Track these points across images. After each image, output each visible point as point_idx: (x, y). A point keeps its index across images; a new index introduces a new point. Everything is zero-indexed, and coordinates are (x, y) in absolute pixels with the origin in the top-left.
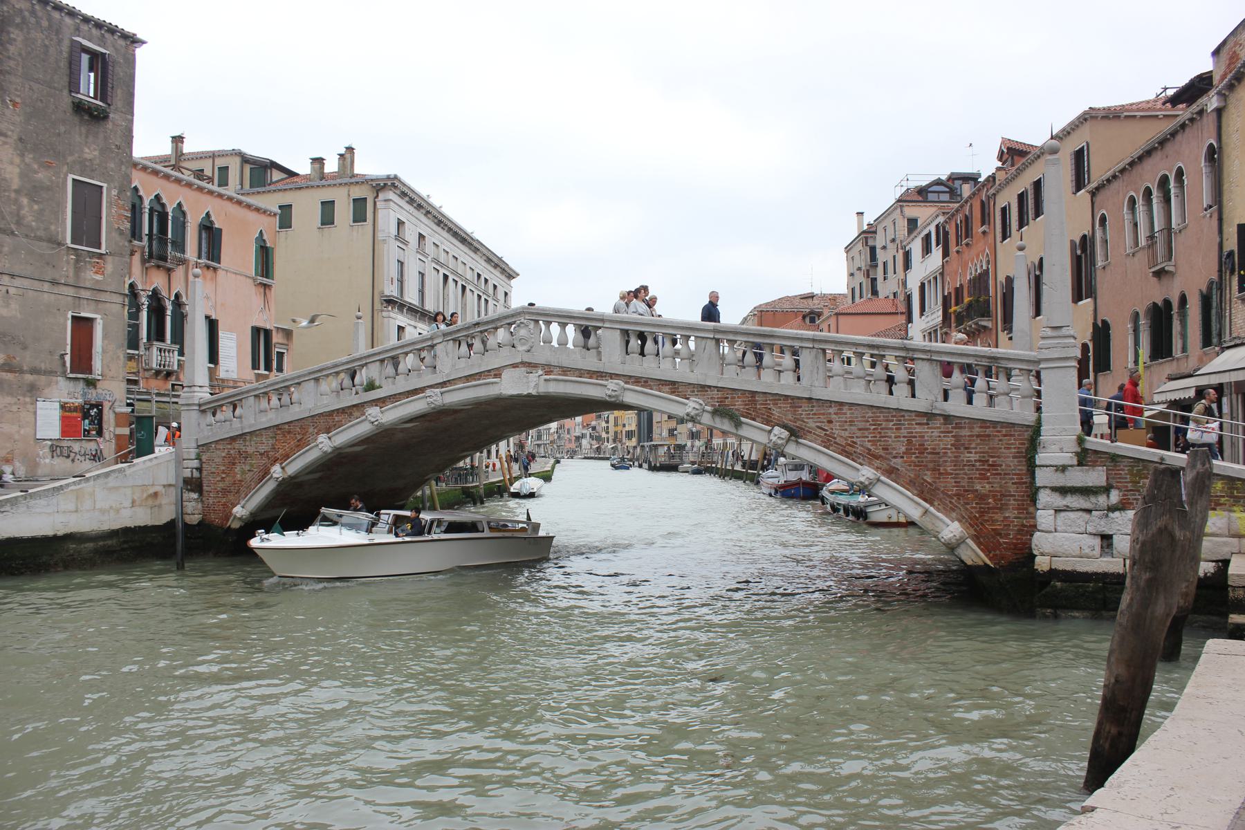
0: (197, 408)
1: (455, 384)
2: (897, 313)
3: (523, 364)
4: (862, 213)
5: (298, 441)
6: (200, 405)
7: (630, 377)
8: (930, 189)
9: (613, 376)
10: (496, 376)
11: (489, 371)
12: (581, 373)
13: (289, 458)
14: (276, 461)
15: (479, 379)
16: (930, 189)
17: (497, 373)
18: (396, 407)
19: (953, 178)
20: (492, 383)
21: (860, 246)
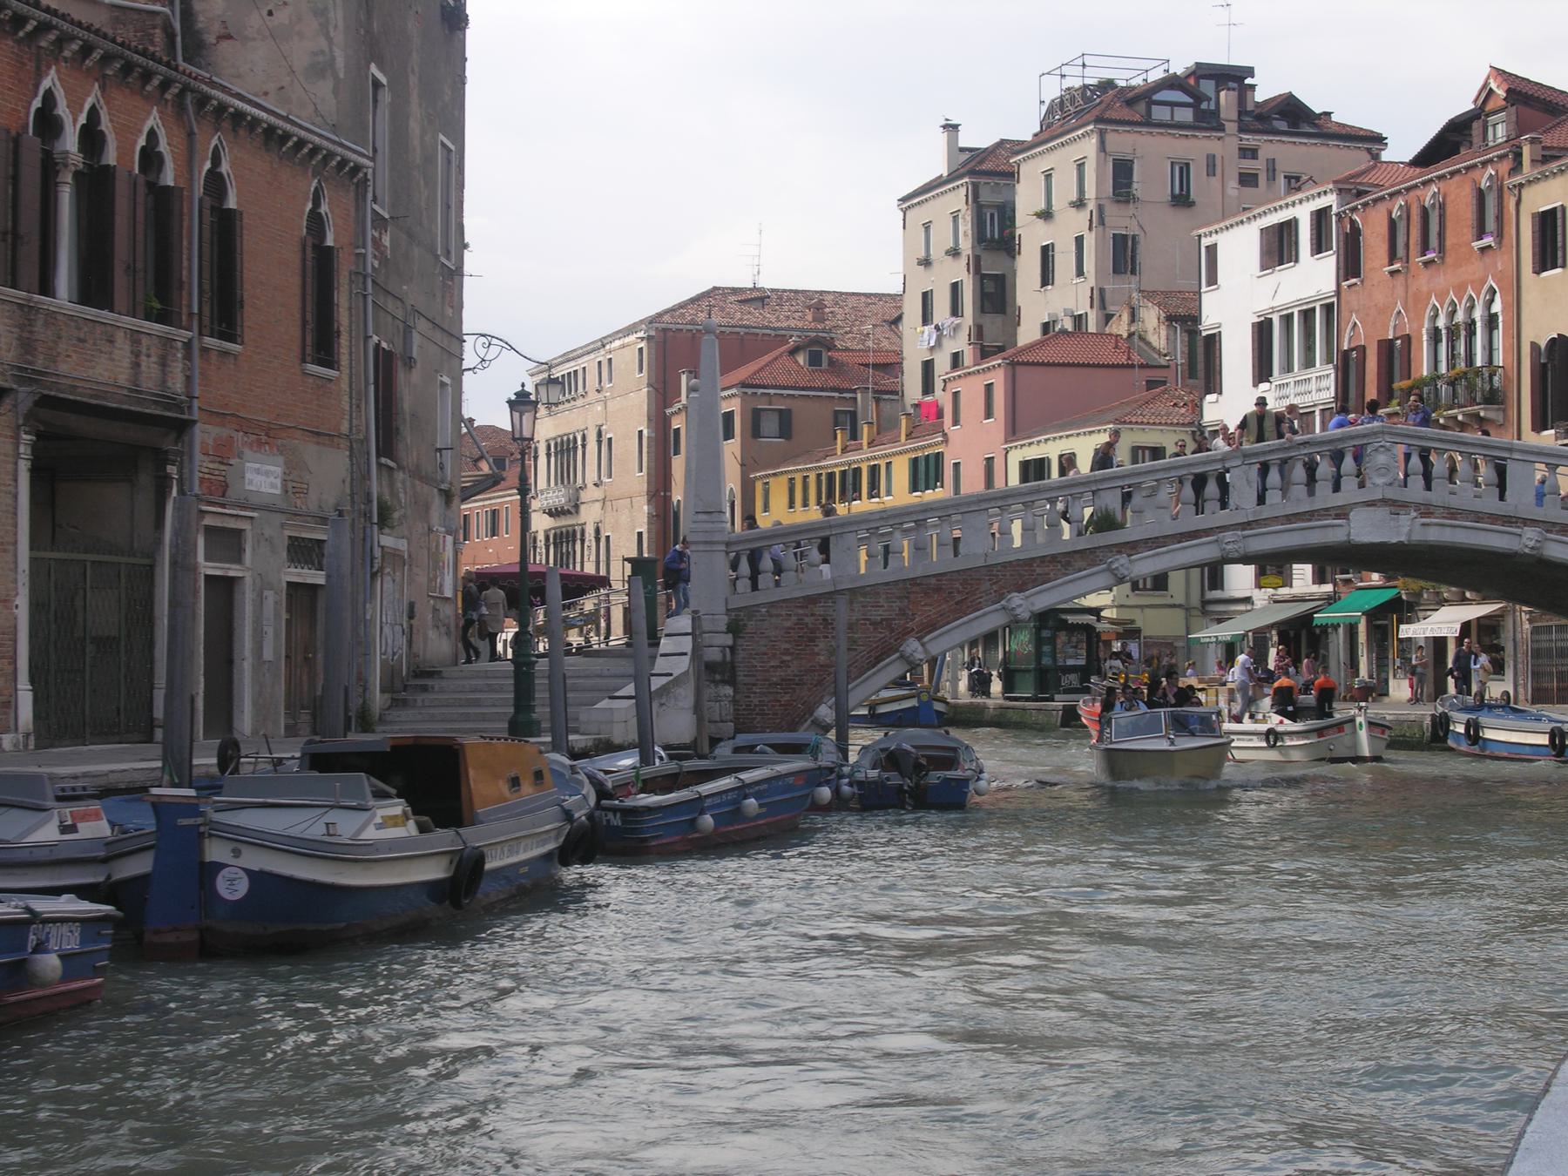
0: (723, 548)
1: (1266, 526)
2: (1133, 366)
3: (1385, 502)
4: (955, 127)
5: (957, 603)
6: (728, 544)
7: (1554, 524)
8: (1156, 97)
9: (1527, 522)
10: (1338, 517)
11: (1327, 509)
12: (1478, 516)
13: (936, 629)
14: (906, 633)
15: (1310, 520)
16: (1156, 97)
17: (1342, 513)
18: (1158, 554)
19: (1203, 71)
20: (1333, 526)
21: (957, 199)
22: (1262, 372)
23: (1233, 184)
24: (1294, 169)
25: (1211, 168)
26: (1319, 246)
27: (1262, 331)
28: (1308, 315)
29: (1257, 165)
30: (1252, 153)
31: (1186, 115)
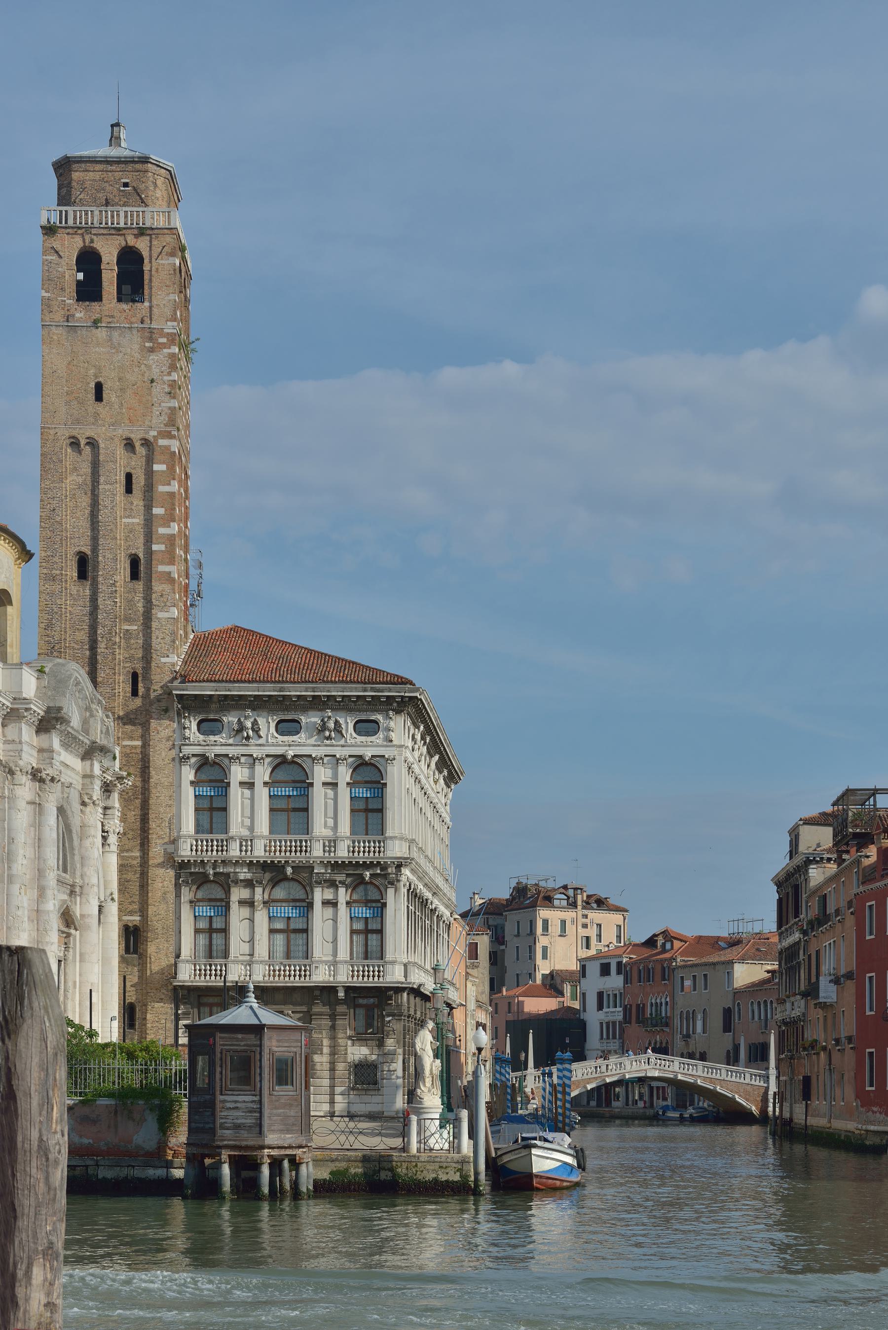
22: (600, 1007)
23: (580, 927)
24: (599, 922)
25: (573, 921)
26: (619, 972)
27: (600, 995)
28: (615, 995)
29: (587, 921)
30: (586, 916)
31: (564, 903)
